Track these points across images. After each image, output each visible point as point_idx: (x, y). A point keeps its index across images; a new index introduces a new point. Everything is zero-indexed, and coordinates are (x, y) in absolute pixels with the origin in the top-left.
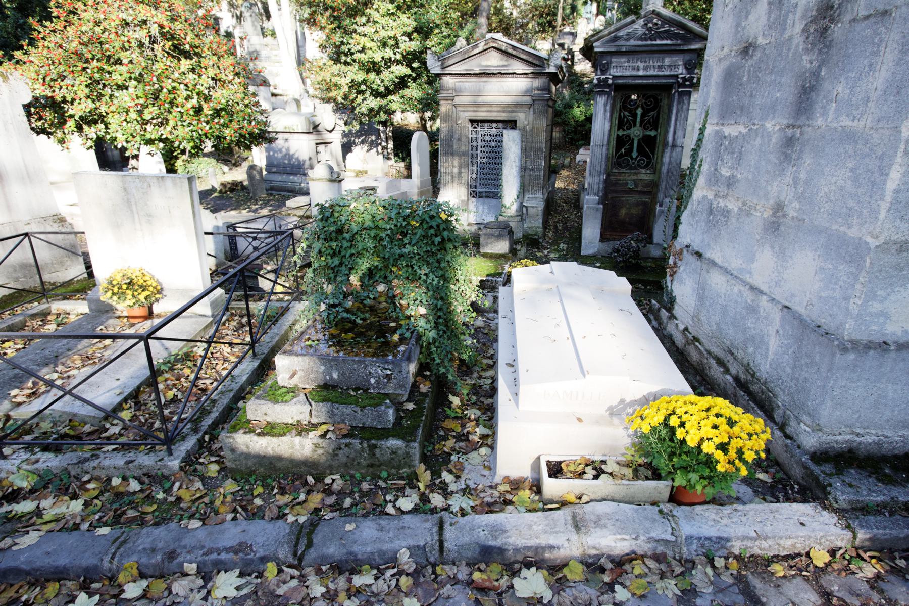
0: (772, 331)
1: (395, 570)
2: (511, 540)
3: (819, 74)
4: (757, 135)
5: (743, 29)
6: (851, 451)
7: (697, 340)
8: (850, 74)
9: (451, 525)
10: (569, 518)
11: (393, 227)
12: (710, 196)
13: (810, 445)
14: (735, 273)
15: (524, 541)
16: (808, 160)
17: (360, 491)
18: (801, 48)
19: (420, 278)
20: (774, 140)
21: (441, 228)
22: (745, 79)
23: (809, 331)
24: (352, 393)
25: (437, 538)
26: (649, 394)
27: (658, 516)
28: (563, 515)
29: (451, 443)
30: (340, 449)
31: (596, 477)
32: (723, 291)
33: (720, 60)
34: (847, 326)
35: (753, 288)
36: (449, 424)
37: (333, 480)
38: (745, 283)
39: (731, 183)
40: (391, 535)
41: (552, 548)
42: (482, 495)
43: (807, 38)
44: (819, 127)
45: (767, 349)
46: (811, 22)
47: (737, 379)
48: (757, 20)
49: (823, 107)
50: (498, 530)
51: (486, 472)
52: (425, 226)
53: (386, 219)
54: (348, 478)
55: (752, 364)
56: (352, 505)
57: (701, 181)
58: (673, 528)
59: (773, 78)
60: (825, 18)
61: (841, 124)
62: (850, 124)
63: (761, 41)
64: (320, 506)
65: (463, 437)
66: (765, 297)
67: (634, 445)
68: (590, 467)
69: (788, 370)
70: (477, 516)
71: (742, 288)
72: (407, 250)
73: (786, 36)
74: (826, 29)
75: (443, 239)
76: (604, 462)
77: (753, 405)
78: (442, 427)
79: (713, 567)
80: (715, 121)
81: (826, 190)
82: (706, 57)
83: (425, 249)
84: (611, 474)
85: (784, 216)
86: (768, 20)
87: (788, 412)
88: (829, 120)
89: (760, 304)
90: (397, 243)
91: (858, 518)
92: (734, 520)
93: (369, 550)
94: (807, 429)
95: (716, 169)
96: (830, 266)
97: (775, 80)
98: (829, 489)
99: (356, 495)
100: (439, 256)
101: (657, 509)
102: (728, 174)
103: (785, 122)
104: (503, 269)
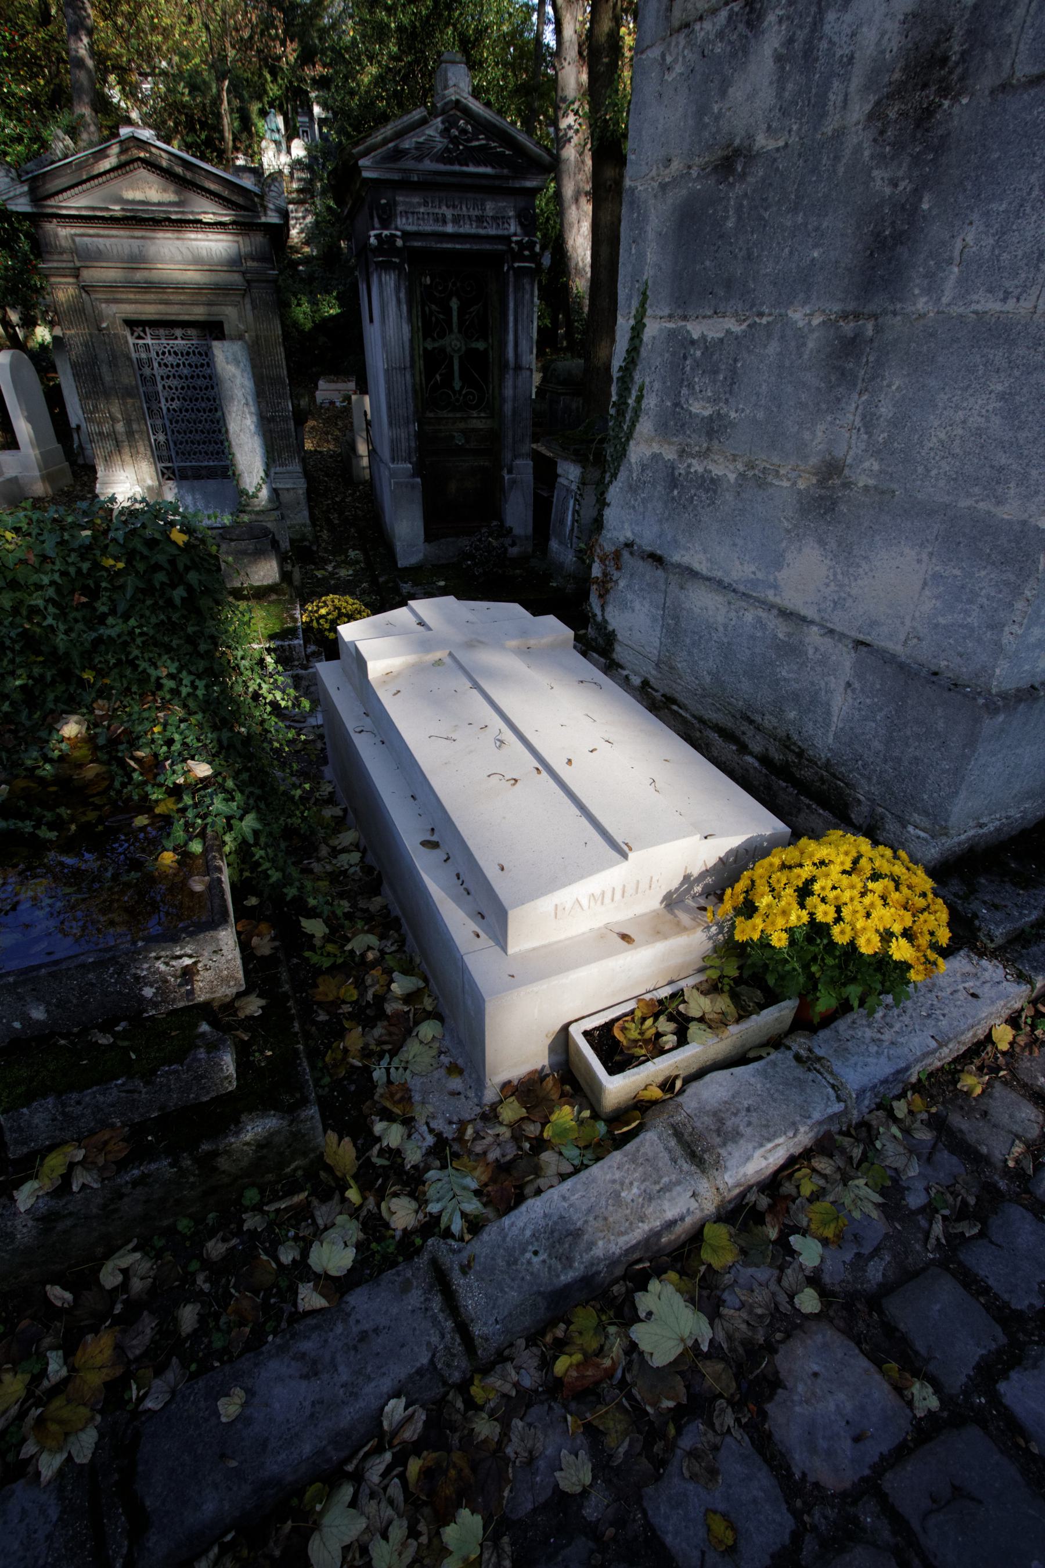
0: (837, 684)
1: (388, 1456)
2: (599, 1250)
3: (916, 207)
4: (769, 336)
5: (717, 118)
6: (971, 849)
7: (674, 701)
8: (994, 206)
9: (465, 1270)
10: (673, 1143)
11: (56, 577)
12: (669, 454)
13: (929, 857)
14: (741, 588)
15: (625, 1238)
16: (896, 381)
17: (207, 1264)
18: (867, 153)
19: (160, 686)
20: (811, 345)
21: (181, 567)
22: (730, 224)
23: (907, 680)
24: (105, 1040)
25: (449, 1324)
26: (728, 854)
27: (799, 1072)
28: (652, 1141)
29: (354, 1039)
30: (121, 1196)
31: (682, 1040)
32: (721, 619)
33: (663, 187)
34: (998, 671)
35: (786, 614)
36: (327, 989)
37: (125, 1272)
38: (770, 607)
39: (714, 428)
40: (344, 1375)
41: (671, 1224)
42: (478, 1149)
43: (882, 133)
44: (922, 316)
45: (828, 713)
46: (889, 96)
47: (764, 760)
48: (751, 97)
49: (930, 275)
50: (563, 1236)
51: (456, 1083)
52: (141, 567)
53: (33, 559)
54: (159, 1242)
55: (795, 737)
56: (202, 1319)
57: (645, 427)
58: (833, 1086)
59: (800, 219)
60: (925, 86)
61: (974, 307)
62: (998, 306)
63: (762, 141)
64: (119, 1371)
65: (370, 1013)
66: (815, 629)
67: (715, 949)
68: (662, 1019)
69: (877, 745)
70: (506, 1221)
71: (763, 615)
72: (113, 628)
73: (829, 130)
74: (929, 112)
75: (190, 589)
76: (678, 996)
77: (807, 801)
78: (320, 1004)
79: (896, 1120)
80: (667, 312)
81: (942, 436)
82: (628, 183)
83: (154, 620)
84: (701, 1020)
85: (847, 485)
86: (779, 96)
87: (880, 810)
88: (945, 300)
89: (807, 640)
90: (78, 615)
91: (1022, 956)
92: (897, 1027)
93: (307, 1449)
94: (922, 834)
95: (677, 404)
96: (957, 572)
97: (806, 225)
98: (977, 922)
99: (200, 1279)
100: (190, 630)
101: (790, 1055)
102: (706, 413)
103: (837, 307)
104: (295, 620)
